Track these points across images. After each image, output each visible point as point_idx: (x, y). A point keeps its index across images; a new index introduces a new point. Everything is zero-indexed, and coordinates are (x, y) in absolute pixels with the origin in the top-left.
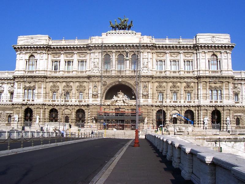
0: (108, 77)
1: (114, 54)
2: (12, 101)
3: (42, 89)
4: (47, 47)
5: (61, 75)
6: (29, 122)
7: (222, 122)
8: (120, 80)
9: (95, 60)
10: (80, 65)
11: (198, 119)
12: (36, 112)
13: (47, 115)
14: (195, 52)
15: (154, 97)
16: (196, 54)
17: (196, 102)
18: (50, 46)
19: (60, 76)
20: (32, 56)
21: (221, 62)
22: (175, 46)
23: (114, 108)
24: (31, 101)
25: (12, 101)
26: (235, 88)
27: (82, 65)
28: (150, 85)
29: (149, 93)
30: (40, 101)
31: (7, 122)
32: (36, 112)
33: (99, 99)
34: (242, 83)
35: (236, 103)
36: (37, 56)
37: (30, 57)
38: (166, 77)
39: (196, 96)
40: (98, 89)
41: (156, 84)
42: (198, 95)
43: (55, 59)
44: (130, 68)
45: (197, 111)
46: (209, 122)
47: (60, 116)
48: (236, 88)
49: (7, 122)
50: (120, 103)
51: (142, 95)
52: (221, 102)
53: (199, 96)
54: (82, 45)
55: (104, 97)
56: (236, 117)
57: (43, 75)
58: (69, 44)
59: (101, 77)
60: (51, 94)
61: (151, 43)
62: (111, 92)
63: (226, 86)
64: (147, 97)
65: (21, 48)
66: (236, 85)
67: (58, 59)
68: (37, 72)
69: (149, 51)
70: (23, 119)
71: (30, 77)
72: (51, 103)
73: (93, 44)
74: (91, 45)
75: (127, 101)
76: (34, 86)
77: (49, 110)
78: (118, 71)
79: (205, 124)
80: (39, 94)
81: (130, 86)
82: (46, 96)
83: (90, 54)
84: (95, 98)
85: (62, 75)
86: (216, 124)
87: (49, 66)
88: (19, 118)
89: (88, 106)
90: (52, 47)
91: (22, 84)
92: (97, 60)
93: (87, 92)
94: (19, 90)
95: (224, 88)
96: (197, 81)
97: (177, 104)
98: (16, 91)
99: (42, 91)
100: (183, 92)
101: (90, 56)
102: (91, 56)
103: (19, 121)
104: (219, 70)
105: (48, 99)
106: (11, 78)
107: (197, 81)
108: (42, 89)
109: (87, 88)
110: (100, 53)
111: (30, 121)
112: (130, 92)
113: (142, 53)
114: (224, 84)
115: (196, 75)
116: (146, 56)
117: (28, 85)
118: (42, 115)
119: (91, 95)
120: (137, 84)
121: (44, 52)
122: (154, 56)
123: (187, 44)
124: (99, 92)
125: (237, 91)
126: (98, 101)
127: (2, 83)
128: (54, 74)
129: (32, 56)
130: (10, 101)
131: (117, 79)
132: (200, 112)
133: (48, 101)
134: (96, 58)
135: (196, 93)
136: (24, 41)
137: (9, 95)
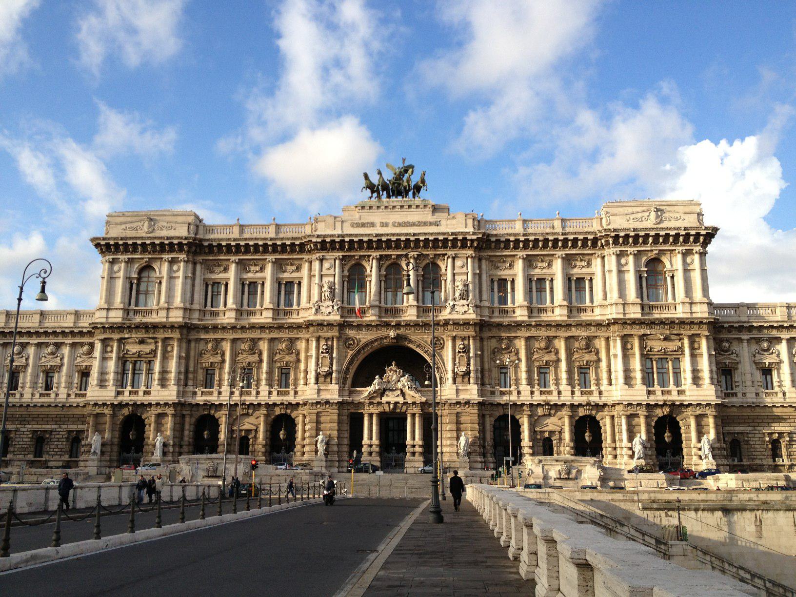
0: (359, 326)
2: (84, 395)
6: (132, 455)
8: (392, 334)
9: (325, 279)
10: (283, 292)
11: (614, 441)
13: (187, 433)
15: (487, 381)
16: (603, 258)
17: (604, 394)
18: (201, 240)
19: (228, 324)
21: (675, 278)
22: (541, 238)
23: (377, 411)
24: (141, 393)
29: (472, 368)
31: (66, 457)
33: (335, 387)
34: (743, 337)
35: (727, 395)
37: (141, 271)
44: (420, 301)
45: (608, 421)
47: (222, 436)
48: (728, 351)
49: (67, 456)
50: (391, 398)
51: (450, 375)
52: (680, 392)
53: (613, 377)
54: (288, 239)
55: (349, 381)
56: (729, 439)
58: (254, 236)
60: (201, 376)
62: (369, 366)
64: (466, 380)
65: (116, 245)
66: (726, 344)
69: (470, 252)
70: (116, 448)
71: (138, 327)
73: (318, 236)
74: (314, 240)
77: (193, 420)
78: (387, 310)
79: (636, 456)
82: (186, 379)
85: (233, 321)
87: (196, 296)
88: (103, 445)
90: (206, 244)
92: (332, 279)
97: (553, 399)
103: (103, 453)
104: (670, 300)
105: (190, 389)
106: (84, 330)
109: (302, 356)
110: (337, 261)
112: (419, 368)
115: (599, 318)
116: (463, 267)
117: (133, 349)
119: (312, 376)
120: (438, 344)
121: (182, 256)
123: (575, 233)
125: (727, 361)
131: (383, 332)
132: (616, 420)
133: (190, 394)
134: (327, 275)
136: (124, 226)
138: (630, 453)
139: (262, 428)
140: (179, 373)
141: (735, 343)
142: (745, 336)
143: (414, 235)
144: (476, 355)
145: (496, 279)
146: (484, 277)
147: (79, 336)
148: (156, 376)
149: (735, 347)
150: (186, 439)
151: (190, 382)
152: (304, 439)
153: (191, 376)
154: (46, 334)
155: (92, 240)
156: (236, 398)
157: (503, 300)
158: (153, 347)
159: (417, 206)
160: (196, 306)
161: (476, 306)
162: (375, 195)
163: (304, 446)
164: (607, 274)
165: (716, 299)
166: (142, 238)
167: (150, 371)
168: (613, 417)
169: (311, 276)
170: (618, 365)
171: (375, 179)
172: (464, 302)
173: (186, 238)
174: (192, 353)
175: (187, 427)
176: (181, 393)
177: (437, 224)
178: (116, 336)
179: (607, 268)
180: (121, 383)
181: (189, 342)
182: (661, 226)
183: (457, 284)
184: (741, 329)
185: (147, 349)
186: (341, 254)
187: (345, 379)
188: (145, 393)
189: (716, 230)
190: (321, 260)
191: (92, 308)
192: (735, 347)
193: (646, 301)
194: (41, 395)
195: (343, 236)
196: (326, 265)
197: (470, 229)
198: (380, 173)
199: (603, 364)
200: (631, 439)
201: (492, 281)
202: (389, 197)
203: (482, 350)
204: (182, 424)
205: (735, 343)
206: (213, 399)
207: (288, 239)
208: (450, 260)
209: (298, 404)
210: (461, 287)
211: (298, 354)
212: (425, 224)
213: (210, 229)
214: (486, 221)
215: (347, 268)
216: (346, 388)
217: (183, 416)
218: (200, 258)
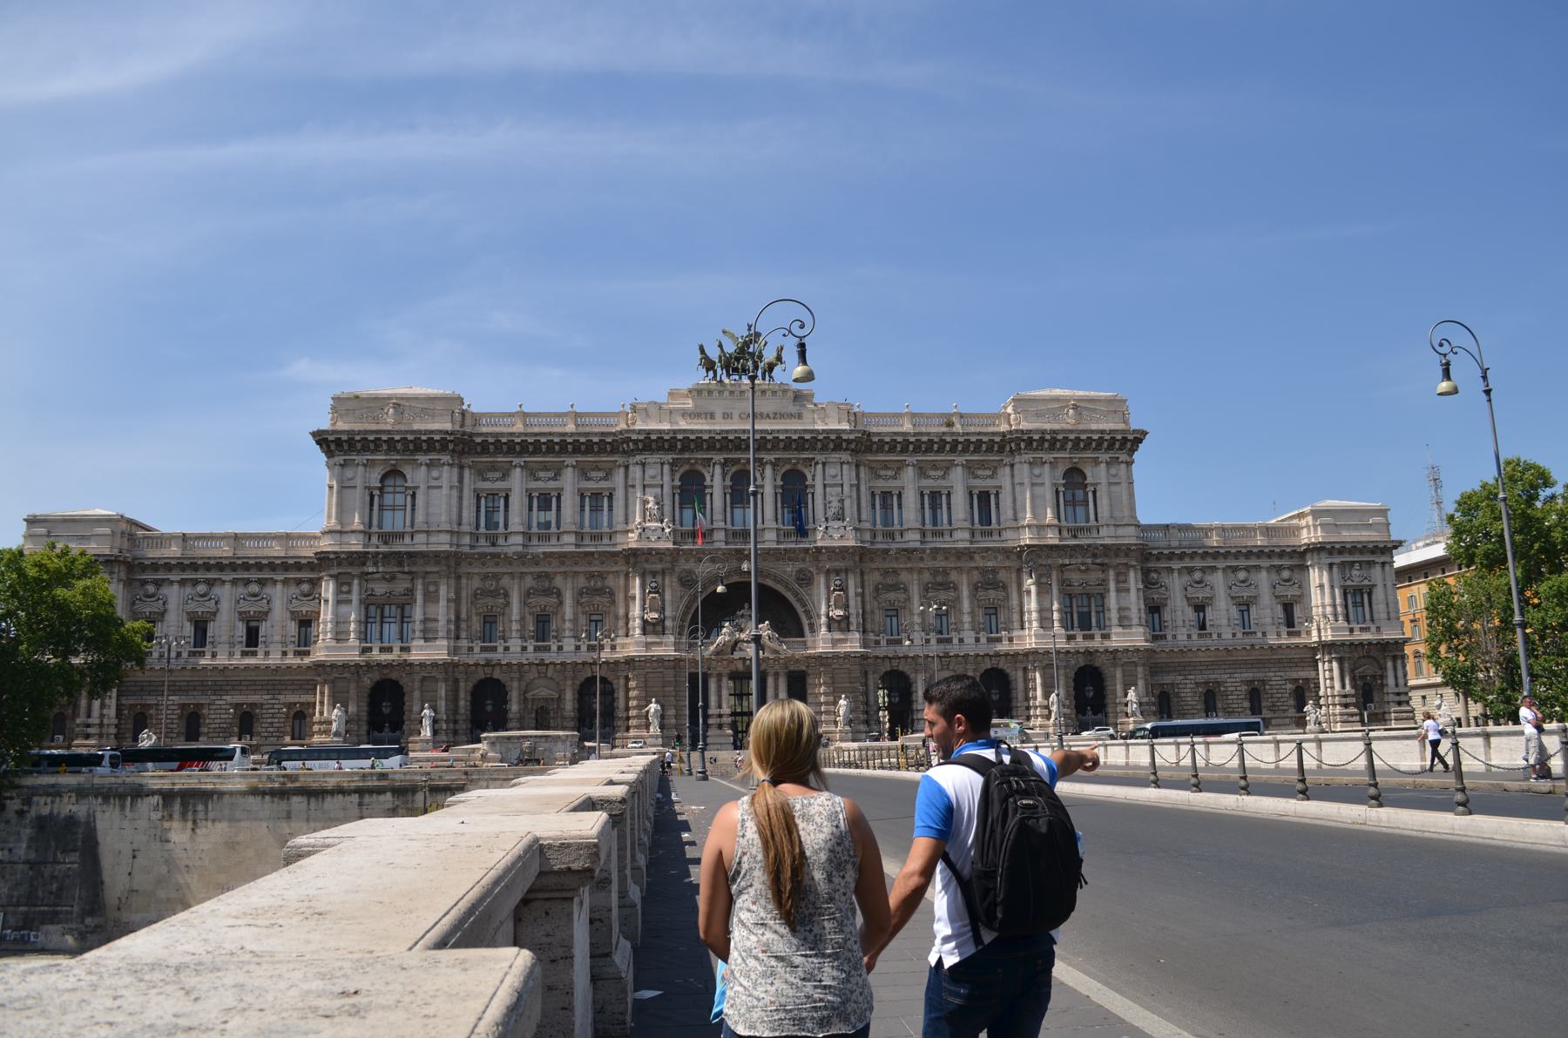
0: (698, 556)
1: (718, 470)
3: (443, 603)
4: (456, 442)
5: (514, 549)
6: (386, 733)
7: (1110, 709)
10: (587, 508)
12: (417, 694)
13: (464, 703)
14: (1007, 460)
15: (869, 626)
16: (1012, 466)
18: (471, 435)
20: (394, 473)
23: (727, 671)
25: (307, 653)
26: (1148, 583)
27: (596, 509)
28: (852, 583)
29: (852, 610)
30: (435, 652)
32: (417, 694)
35: (1155, 638)
36: (417, 476)
37: (384, 478)
38: (909, 552)
39: (1016, 617)
40: (663, 601)
41: (874, 578)
42: (1022, 613)
43: (487, 485)
45: (1020, 674)
46: (1067, 711)
47: (514, 707)
51: (823, 619)
57: (446, 548)
59: (674, 555)
60: (477, 625)
61: (851, 432)
62: (714, 610)
63: (1118, 582)
65: (351, 442)
66: (1155, 575)
67: (499, 485)
68: (420, 538)
69: (846, 456)
70: (365, 728)
71: (387, 556)
72: (479, 657)
73: (640, 432)
74: (634, 437)
75: (774, 645)
76: (410, 592)
78: (735, 534)
80: (430, 625)
81: (780, 588)
82: (458, 628)
83: (627, 467)
84: (655, 633)
86: (1090, 716)
87: (465, 514)
89: (630, 662)
90: (479, 440)
91: (355, 587)
93: (621, 612)
94: (344, 608)
95: (1112, 586)
96: (1016, 564)
97: (954, 649)
98: (327, 614)
99: (442, 611)
100: (966, 605)
101: (626, 477)
102: (631, 475)
104: (1092, 522)
105: (464, 643)
107: (1016, 564)
108: (443, 603)
109: (620, 597)
110: (666, 468)
111: (393, 731)
113: (820, 467)
114: (1112, 573)
117: (380, 588)
118: (442, 705)
119: (636, 623)
120: (805, 580)
121: (446, 458)
122: (862, 475)
124: (668, 613)
126: (666, 648)
127: (262, 583)
128: (484, 546)
129: (394, 473)
130: (297, 653)
135: (1017, 609)
137: (293, 628)
138: (1046, 712)
139: (569, 696)
140: (449, 621)
141: (1164, 574)
142: (1176, 565)
143: (773, 431)
144: (857, 595)
145: (878, 492)
146: (863, 488)
147: (305, 571)
148: (418, 626)
149: (1165, 579)
150: (462, 711)
151: (463, 635)
152: (627, 709)
153: (463, 625)
154: (246, 567)
155: (314, 434)
156: (531, 656)
157: (887, 521)
158: (409, 585)
159: (774, 393)
160: (465, 528)
161: (855, 529)
162: (711, 374)
163: (628, 718)
164: (1018, 488)
165: (1143, 522)
166: (389, 432)
167: (404, 619)
168: (1025, 669)
169: (628, 487)
170: (1032, 604)
171: (714, 354)
172: (840, 523)
173: (452, 433)
174: (464, 594)
175: (462, 695)
176: (454, 651)
177: (800, 416)
178: (355, 571)
179: (1017, 480)
180: (364, 636)
181: (458, 578)
182: (1081, 427)
183: (829, 498)
184: (1171, 556)
185: (401, 586)
186: (669, 457)
187: (681, 628)
188: (402, 649)
189: (1145, 433)
190: (643, 465)
191: (317, 531)
192: (1165, 579)
193: (1064, 523)
194: (244, 654)
195: (675, 432)
196: (650, 472)
197: (845, 426)
198: (720, 346)
199: (1015, 602)
200: (1046, 696)
201: (873, 495)
202: (728, 375)
203: (863, 587)
204: (456, 691)
205: (1164, 574)
206: (498, 656)
207: (596, 434)
208: (820, 467)
209: (617, 663)
210: (835, 504)
211: (612, 594)
212: (782, 416)
213: (477, 418)
214: (863, 414)
215: (678, 476)
216: (684, 639)
217: (457, 681)
218: (467, 460)
